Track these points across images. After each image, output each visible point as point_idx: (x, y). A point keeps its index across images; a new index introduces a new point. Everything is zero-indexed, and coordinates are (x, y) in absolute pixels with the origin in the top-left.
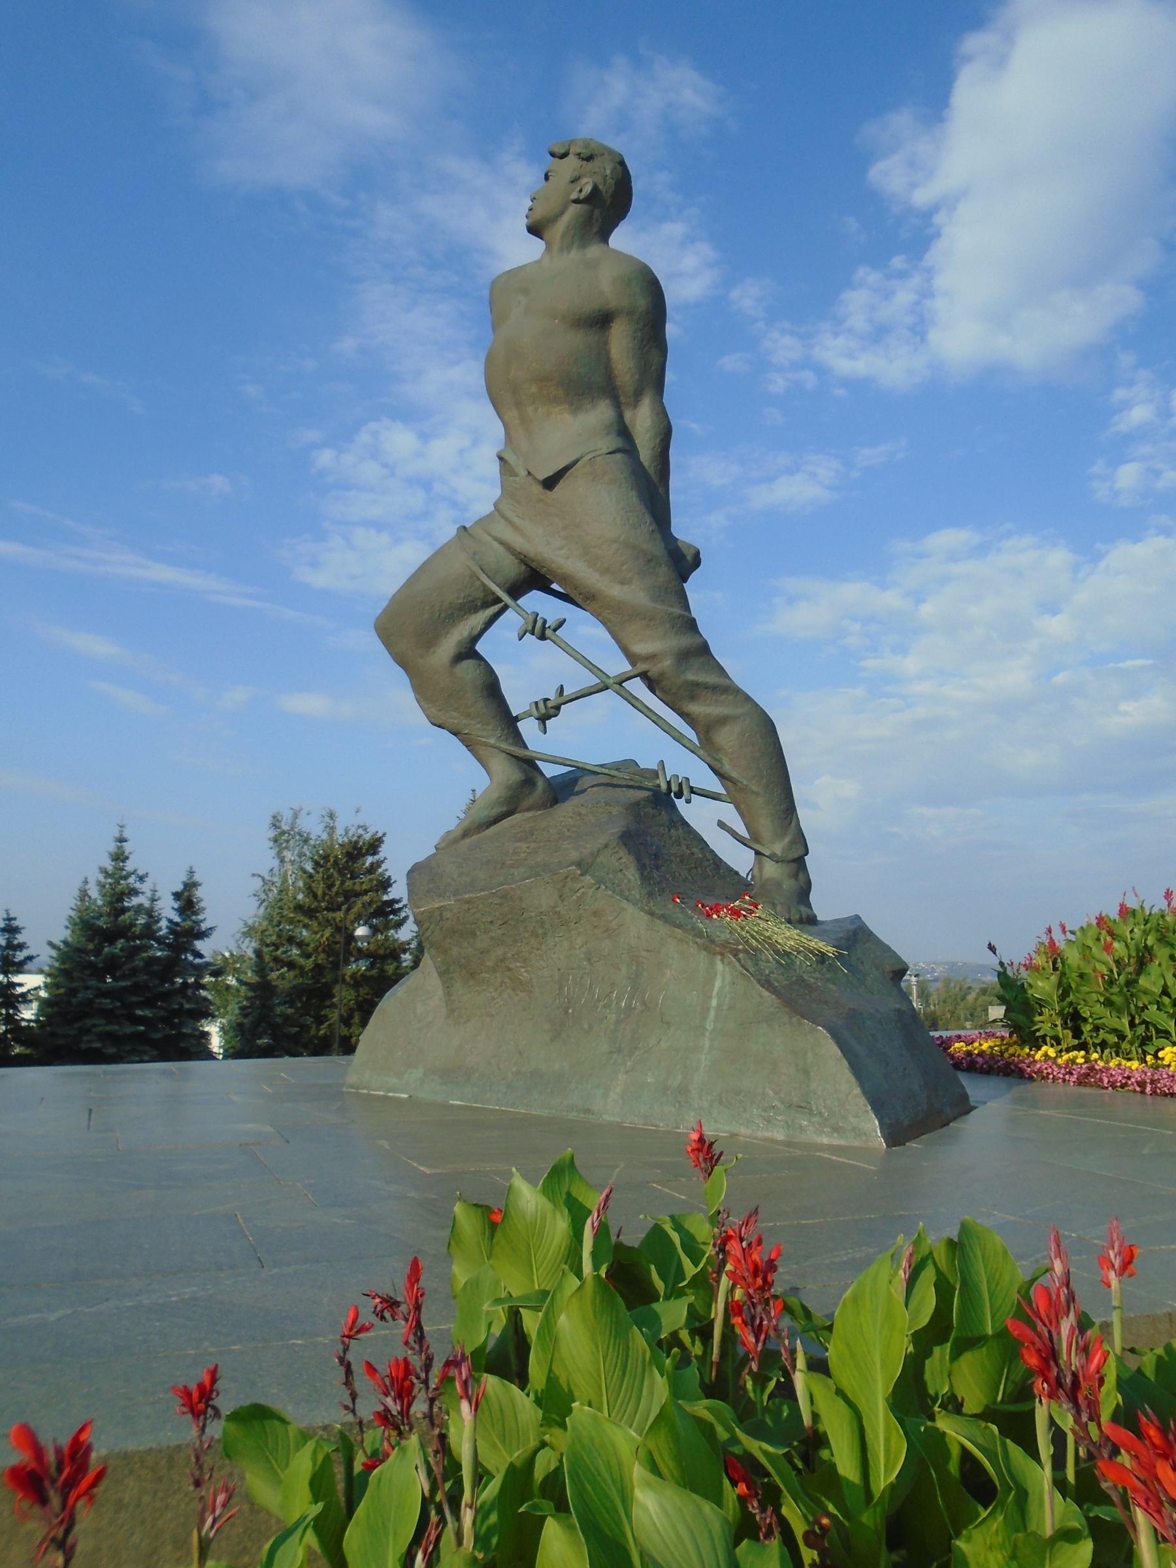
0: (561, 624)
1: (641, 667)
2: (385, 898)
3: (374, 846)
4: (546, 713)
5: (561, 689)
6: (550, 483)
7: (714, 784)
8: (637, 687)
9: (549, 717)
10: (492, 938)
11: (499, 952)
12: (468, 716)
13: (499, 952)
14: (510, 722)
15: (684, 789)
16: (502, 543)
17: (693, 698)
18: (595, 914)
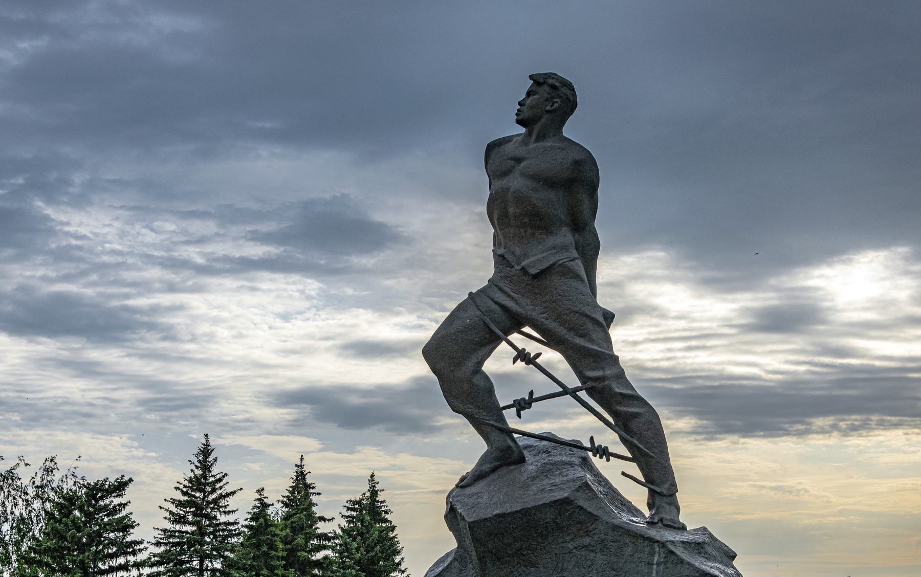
0: (538, 355)
1: (590, 384)
2: (129, 539)
3: (121, 486)
4: (522, 405)
5: (531, 393)
6: (536, 277)
7: (624, 451)
8: (583, 394)
9: (524, 409)
10: (514, 537)
11: (518, 545)
12: (479, 407)
13: (518, 545)
14: (497, 412)
15: (603, 452)
16: (502, 307)
17: (620, 403)
18: (579, 523)
